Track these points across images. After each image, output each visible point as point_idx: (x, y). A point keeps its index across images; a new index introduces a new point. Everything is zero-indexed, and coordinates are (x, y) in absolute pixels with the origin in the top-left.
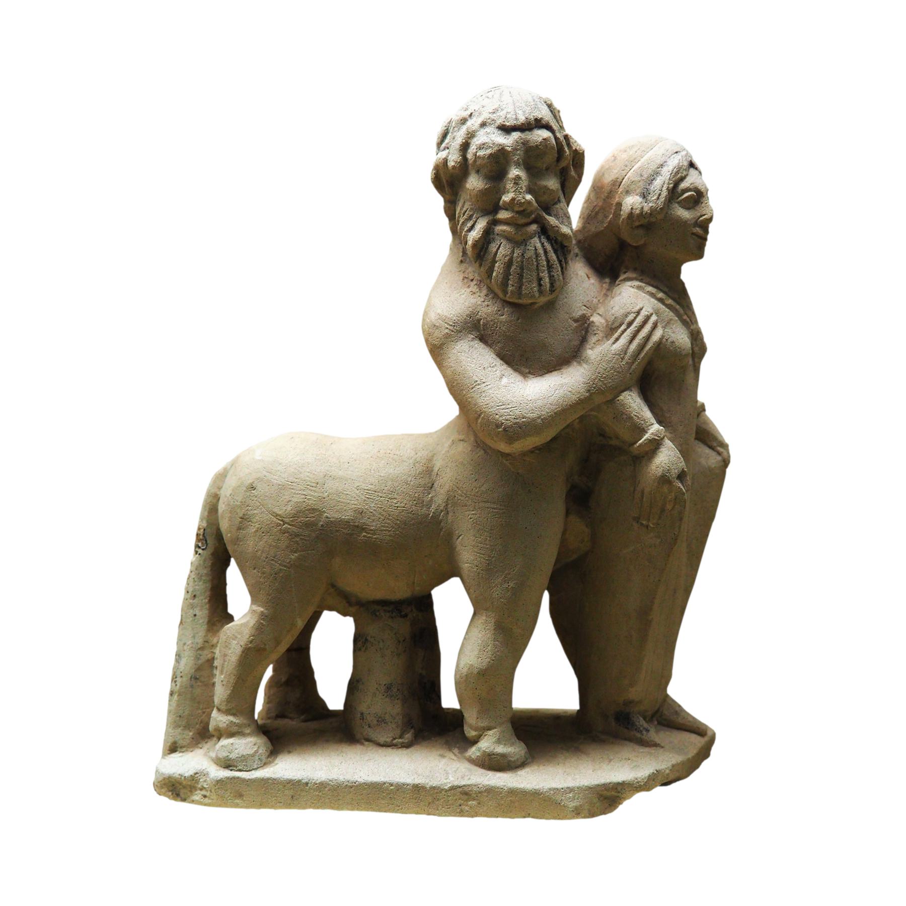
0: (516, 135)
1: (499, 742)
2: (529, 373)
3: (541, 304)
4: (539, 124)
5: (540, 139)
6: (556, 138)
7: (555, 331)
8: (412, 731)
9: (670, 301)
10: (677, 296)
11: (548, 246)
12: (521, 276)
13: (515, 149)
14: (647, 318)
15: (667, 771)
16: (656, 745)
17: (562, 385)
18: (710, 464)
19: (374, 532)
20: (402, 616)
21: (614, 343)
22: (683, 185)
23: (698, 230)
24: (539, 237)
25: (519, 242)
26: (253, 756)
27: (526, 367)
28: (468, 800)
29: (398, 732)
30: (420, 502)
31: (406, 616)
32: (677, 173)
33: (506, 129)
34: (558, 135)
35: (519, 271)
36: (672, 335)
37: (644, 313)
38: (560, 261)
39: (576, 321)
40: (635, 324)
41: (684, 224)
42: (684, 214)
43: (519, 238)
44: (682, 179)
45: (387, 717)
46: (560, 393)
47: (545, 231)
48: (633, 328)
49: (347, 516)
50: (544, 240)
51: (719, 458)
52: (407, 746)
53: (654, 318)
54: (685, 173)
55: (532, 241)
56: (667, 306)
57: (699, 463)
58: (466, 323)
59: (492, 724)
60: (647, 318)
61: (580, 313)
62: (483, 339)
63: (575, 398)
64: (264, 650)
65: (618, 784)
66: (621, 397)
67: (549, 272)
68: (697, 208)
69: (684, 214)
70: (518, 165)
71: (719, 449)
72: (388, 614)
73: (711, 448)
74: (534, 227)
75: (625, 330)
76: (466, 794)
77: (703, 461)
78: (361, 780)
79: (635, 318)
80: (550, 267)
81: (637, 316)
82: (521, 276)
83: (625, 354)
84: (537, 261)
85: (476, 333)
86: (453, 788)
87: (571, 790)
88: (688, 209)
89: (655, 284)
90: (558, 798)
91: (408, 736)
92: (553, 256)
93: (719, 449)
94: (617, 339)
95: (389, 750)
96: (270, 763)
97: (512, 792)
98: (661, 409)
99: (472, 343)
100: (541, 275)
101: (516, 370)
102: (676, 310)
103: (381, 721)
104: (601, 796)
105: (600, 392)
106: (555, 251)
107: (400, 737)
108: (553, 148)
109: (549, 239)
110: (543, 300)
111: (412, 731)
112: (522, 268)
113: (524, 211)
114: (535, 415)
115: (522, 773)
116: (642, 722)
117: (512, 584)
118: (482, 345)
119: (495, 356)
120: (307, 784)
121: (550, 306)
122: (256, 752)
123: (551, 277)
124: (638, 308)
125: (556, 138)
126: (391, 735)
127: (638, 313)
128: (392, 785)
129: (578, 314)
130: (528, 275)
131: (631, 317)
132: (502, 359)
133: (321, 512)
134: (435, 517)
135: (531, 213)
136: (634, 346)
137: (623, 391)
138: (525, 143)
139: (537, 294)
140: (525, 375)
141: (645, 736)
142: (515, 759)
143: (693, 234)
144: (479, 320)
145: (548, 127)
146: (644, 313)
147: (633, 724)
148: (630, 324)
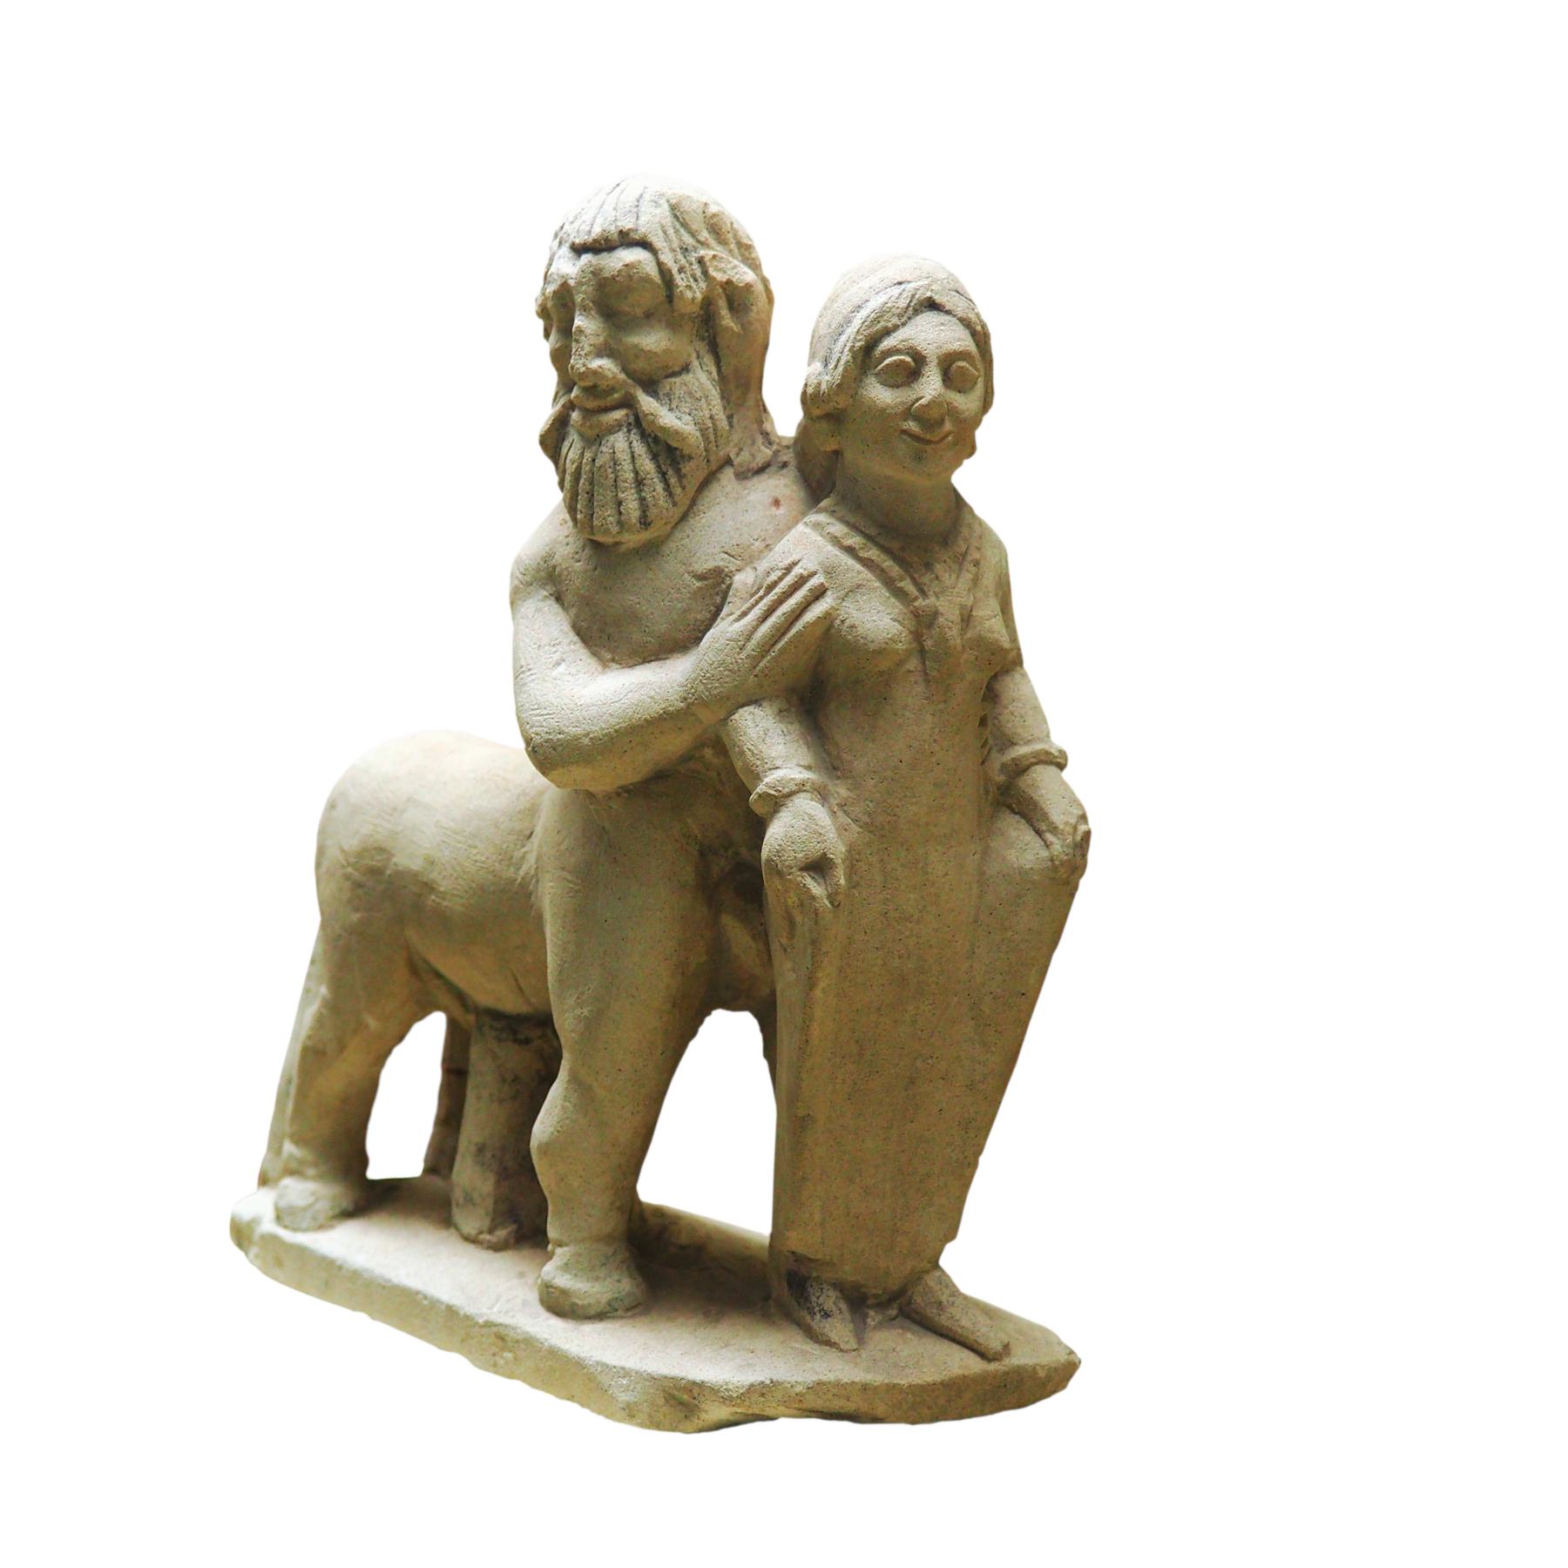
0: (586, 258)
1: (566, 1268)
2: (613, 660)
3: (631, 545)
4: (626, 239)
5: (619, 265)
6: (660, 264)
7: (659, 594)
8: (514, 1227)
9: (873, 553)
10: (895, 545)
11: (640, 448)
12: (591, 494)
13: (580, 284)
14: (802, 581)
15: (799, 1389)
16: (829, 1343)
17: (642, 686)
18: (1022, 862)
19: (443, 896)
20: (515, 1041)
21: (737, 620)
22: (887, 343)
23: (912, 426)
24: (629, 431)
25: (594, 440)
26: (305, 1209)
27: (609, 650)
28: (502, 1349)
29: (487, 1223)
30: (507, 858)
31: (527, 1041)
32: (877, 320)
33: (579, 250)
34: (662, 258)
35: (588, 488)
36: (855, 614)
37: (797, 570)
38: (664, 476)
39: (701, 577)
40: (778, 590)
41: (882, 414)
42: (879, 394)
43: (591, 433)
44: (887, 332)
45: (475, 1195)
46: (635, 697)
47: (639, 424)
48: (771, 597)
49: (415, 865)
50: (635, 437)
51: (1045, 853)
52: (497, 1248)
53: (814, 582)
54: (895, 320)
55: (612, 438)
56: (867, 563)
57: (1004, 859)
58: (538, 570)
59: (565, 1239)
60: (802, 581)
61: (710, 565)
62: (559, 599)
63: (656, 709)
64: (324, 1053)
65: (694, 1383)
66: (736, 716)
67: (639, 491)
68: (915, 386)
69: (879, 394)
70: (585, 309)
71: (1049, 837)
72: (494, 1033)
73: (1039, 833)
74: (619, 414)
75: (761, 598)
76: (501, 1338)
77: (1012, 856)
78: (395, 1280)
79: (781, 579)
80: (639, 483)
81: (785, 575)
82: (591, 494)
83: (749, 638)
84: (615, 471)
85: (550, 589)
86: (488, 1324)
87: (625, 1373)
88: (895, 386)
89: (852, 520)
90: (605, 1380)
91: (501, 1233)
92: (647, 466)
93: (1049, 837)
94: (744, 614)
95: (471, 1248)
96: (331, 1227)
97: (554, 1353)
98: (836, 744)
99: (541, 604)
100: (621, 495)
101: (594, 654)
102: (883, 570)
103: (469, 1200)
104: (674, 1397)
105: (703, 703)
106: (655, 457)
107: (491, 1231)
108: (646, 279)
109: (644, 435)
110: (632, 539)
111: (514, 1227)
112: (591, 483)
113: (595, 386)
114: (579, 731)
115: (589, 1328)
116: (829, 1299)
117: (586, 1012)
118: (556, 608)
119: (567, 627)
120: (340, 1268)
121: (651, 551)
122: (311, 1205)
123: (642, 500)
124: (787, 562)
125: (660, 264)
126: (477, 1225)
127: (789, 569)
128: (425, 1297)
129: (703, 566)
130: (603, 496)
131: (773, 577)
132: (578, 634)
133: (390, 855)
134: (524, 886)
135: (612, 390)
136: (765, 628)
137: (743, 706)
138: (596, 273)
139: (615, 529)
140: (605, 664)
141: (817, 1323)
142: (585, 1302)
143: (904, 432)
144: (554, 567)
145: (645, 244)
146: (797, 570)
147: (807, 1300)
148: (770, 588)
